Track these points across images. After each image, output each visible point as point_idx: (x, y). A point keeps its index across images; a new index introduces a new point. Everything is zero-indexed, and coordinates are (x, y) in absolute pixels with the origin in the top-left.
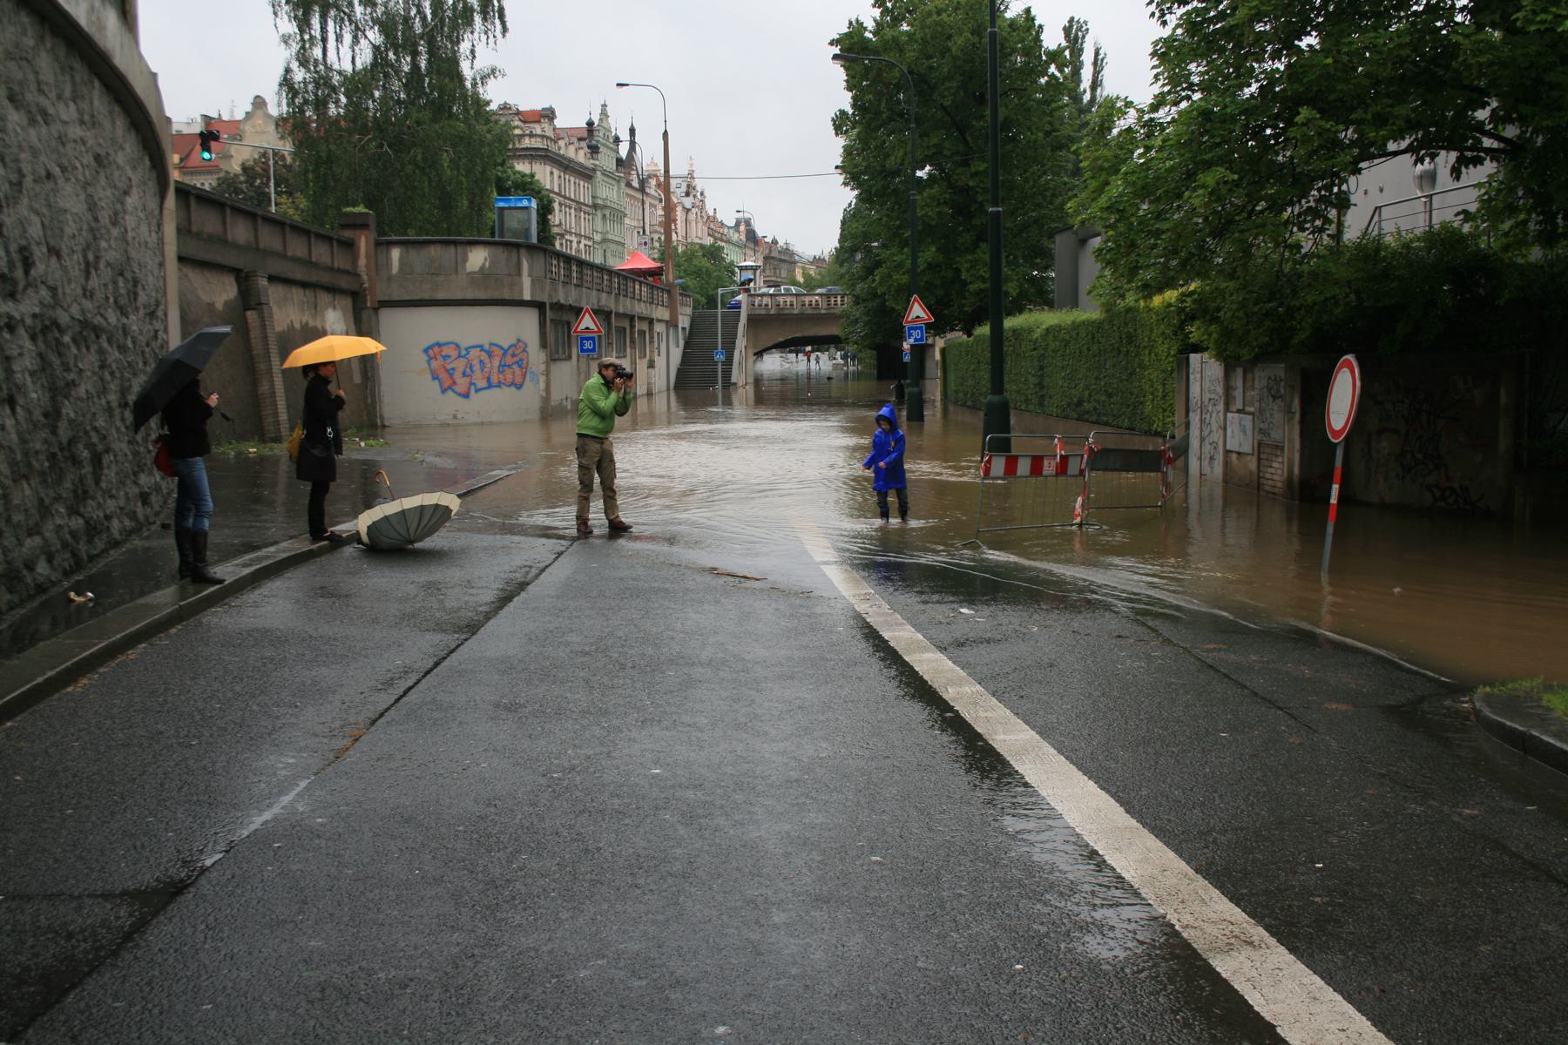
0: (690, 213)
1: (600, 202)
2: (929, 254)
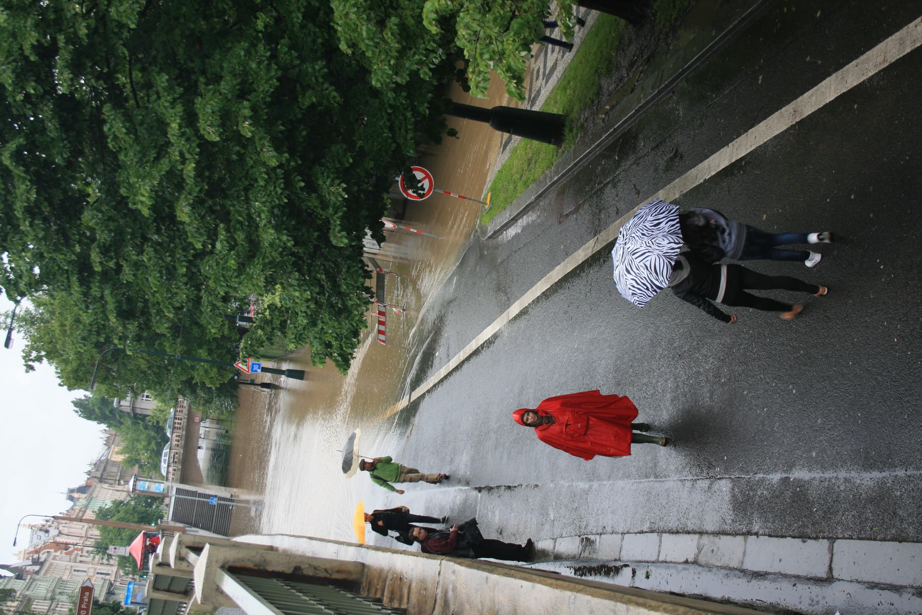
0: (63, 532)
1: (49, 595)
2: (203, 353)
